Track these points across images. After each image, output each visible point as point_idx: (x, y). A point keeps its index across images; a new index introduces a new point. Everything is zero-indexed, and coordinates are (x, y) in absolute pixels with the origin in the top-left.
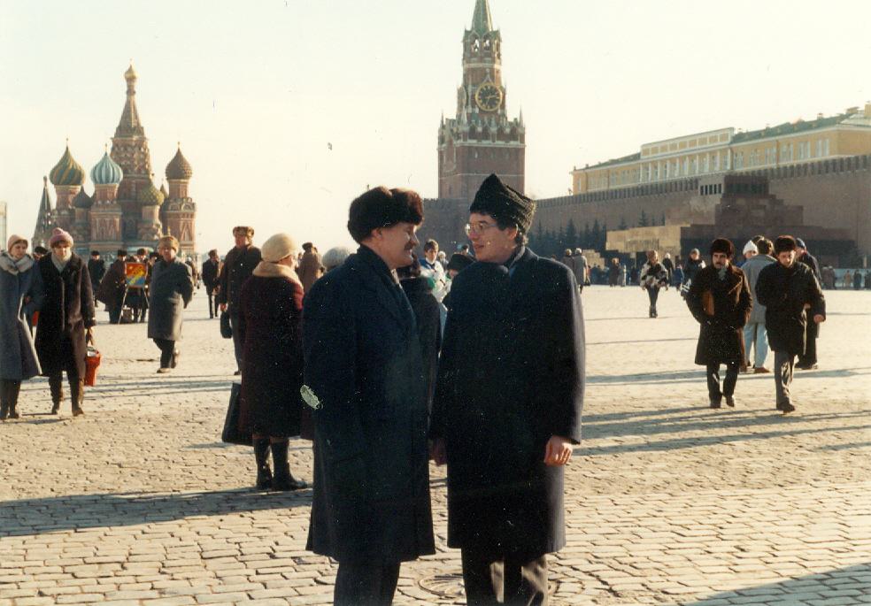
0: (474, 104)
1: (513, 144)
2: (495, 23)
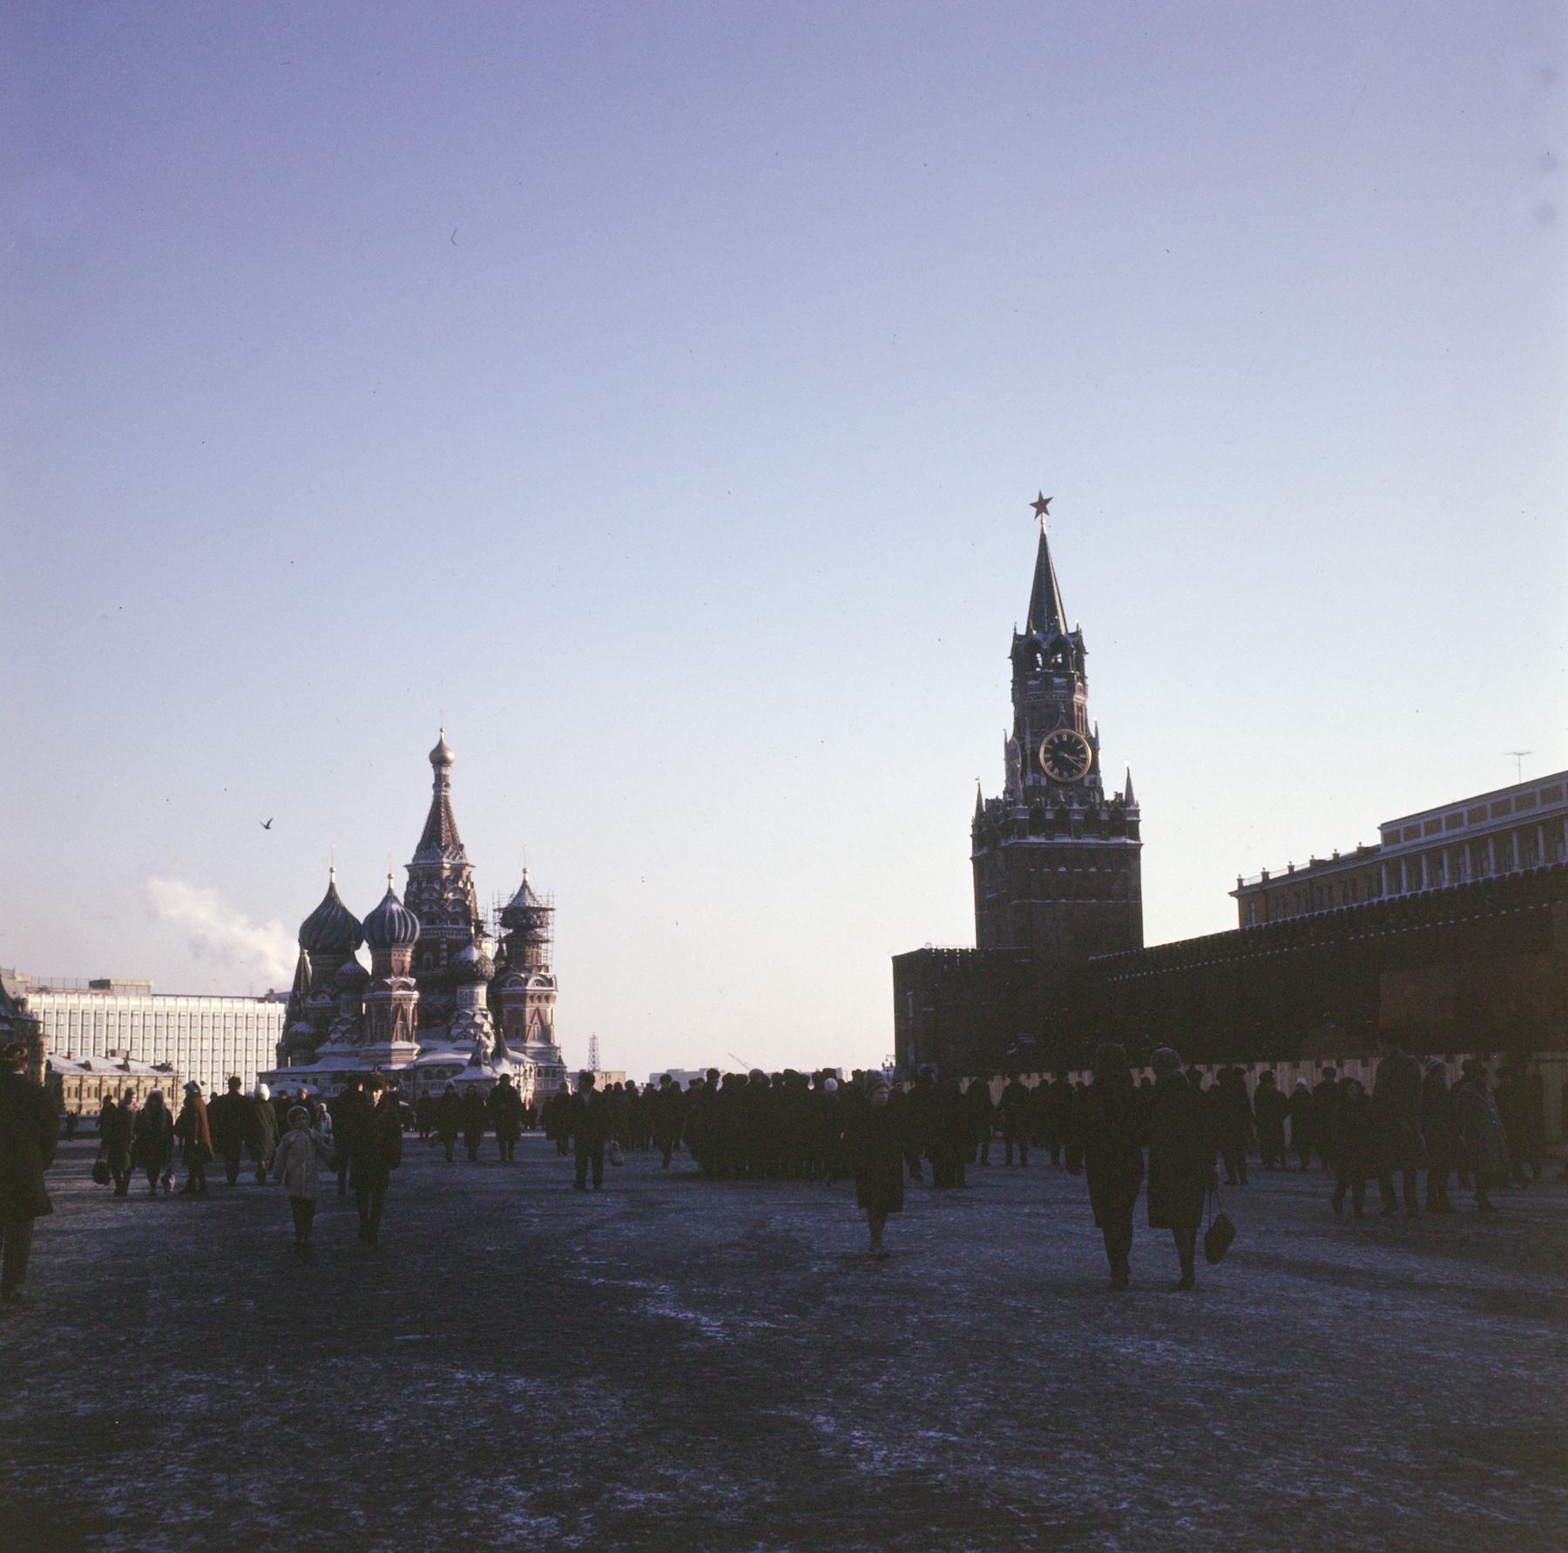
0: (1037, 768)
2: (1073, 615)
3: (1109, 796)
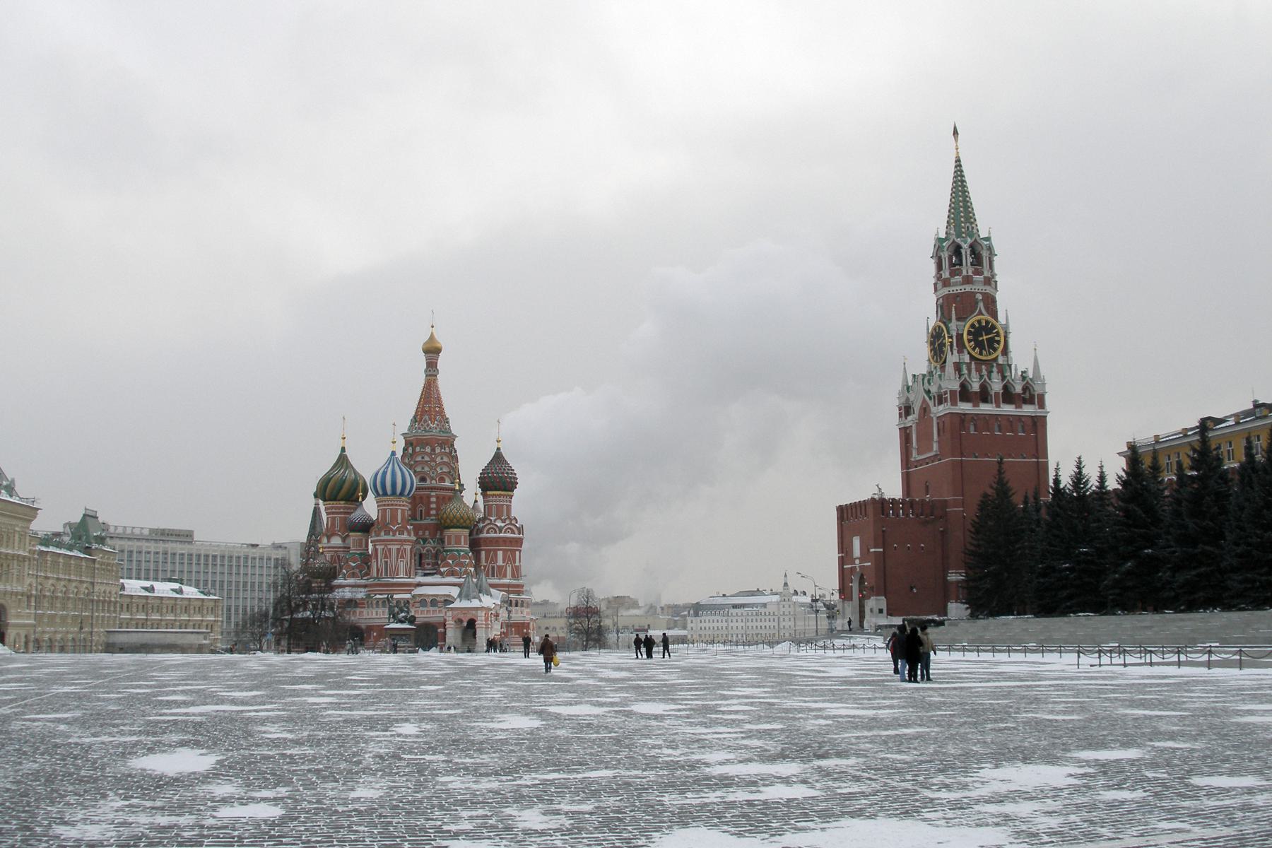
0: (961, 347)
1: (1028, 410)
3: (1015, 374)
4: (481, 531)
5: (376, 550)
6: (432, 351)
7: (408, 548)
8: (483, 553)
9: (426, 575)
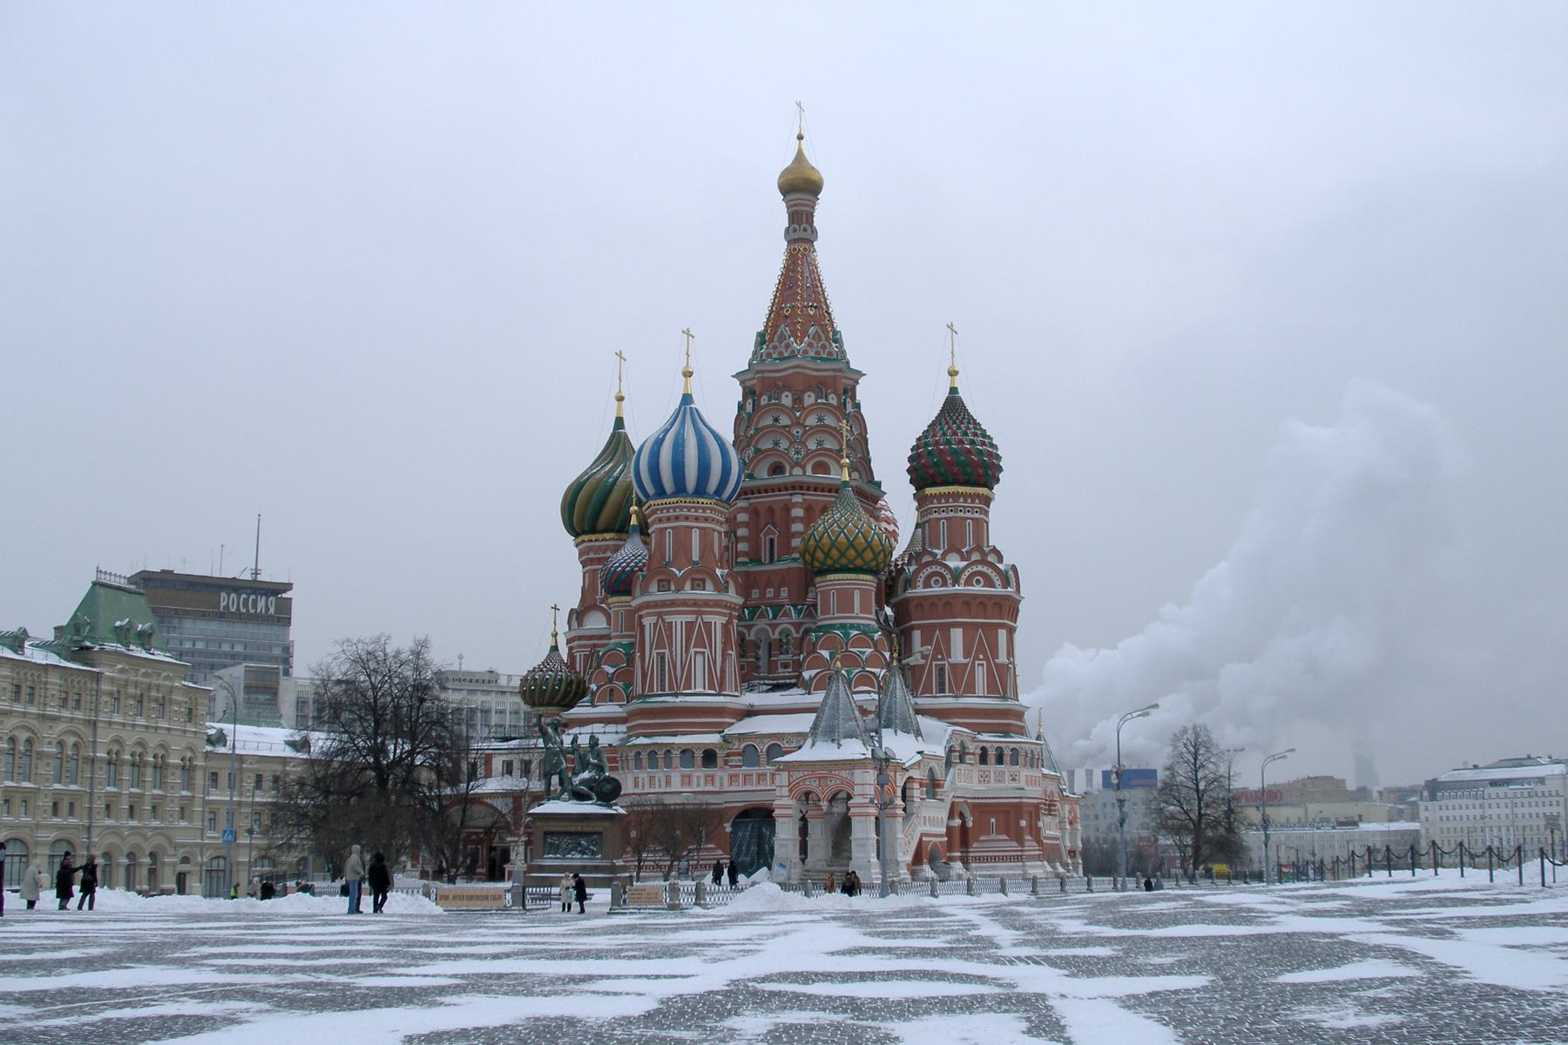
4: (909, 583)
5: (642, 627)
6: (801, 189)
7: (718, 621)
8: (917, 635)
9: (776, 688)
